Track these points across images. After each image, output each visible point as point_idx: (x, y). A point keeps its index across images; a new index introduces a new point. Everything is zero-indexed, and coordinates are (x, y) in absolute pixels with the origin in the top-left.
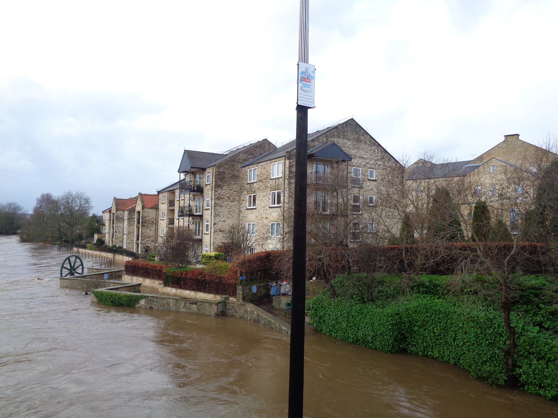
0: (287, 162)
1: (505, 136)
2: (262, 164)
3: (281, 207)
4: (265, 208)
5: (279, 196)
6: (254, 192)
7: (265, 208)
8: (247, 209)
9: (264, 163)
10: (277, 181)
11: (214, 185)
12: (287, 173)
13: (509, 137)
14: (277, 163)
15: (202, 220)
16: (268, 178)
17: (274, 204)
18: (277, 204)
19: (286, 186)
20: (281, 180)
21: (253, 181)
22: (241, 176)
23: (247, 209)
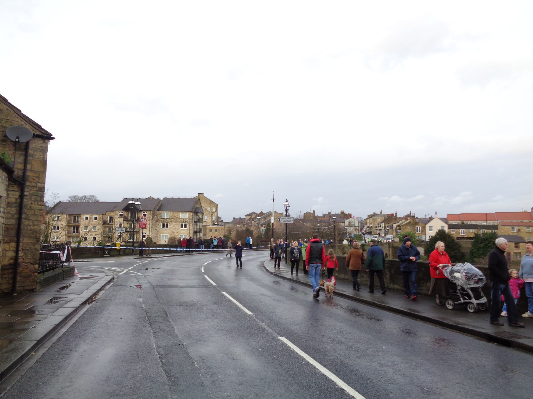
0: (191, 214)
1: (199, 194)
2: (173, 212)
3: (187, 229)
4: (176, 229)
5: (185, 225)
6: (167, 222)
7: (176, 229)
8: (161, 229)
9: (175, 212)
10: (185, 220)
11: (151, 219)
12: (191, 217)
13: (200, 194)
14: (184, 213)
15: (139, 233)
16: (178, 218)
17: (183, 228)
18: (184, 228)
19: (191, 222)
20: (188, 219)
21: (165, 218)
22: (156, 215)
23: (161, 229)
